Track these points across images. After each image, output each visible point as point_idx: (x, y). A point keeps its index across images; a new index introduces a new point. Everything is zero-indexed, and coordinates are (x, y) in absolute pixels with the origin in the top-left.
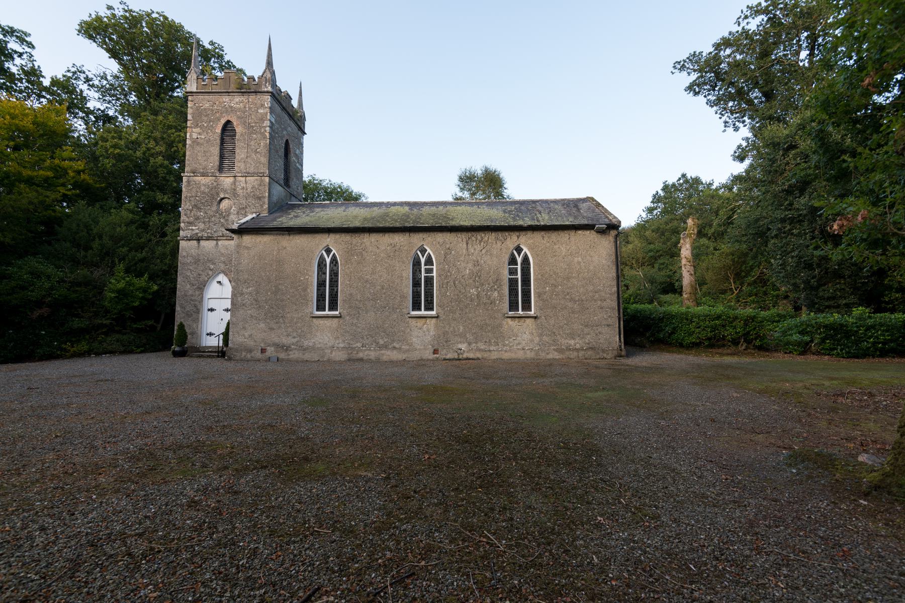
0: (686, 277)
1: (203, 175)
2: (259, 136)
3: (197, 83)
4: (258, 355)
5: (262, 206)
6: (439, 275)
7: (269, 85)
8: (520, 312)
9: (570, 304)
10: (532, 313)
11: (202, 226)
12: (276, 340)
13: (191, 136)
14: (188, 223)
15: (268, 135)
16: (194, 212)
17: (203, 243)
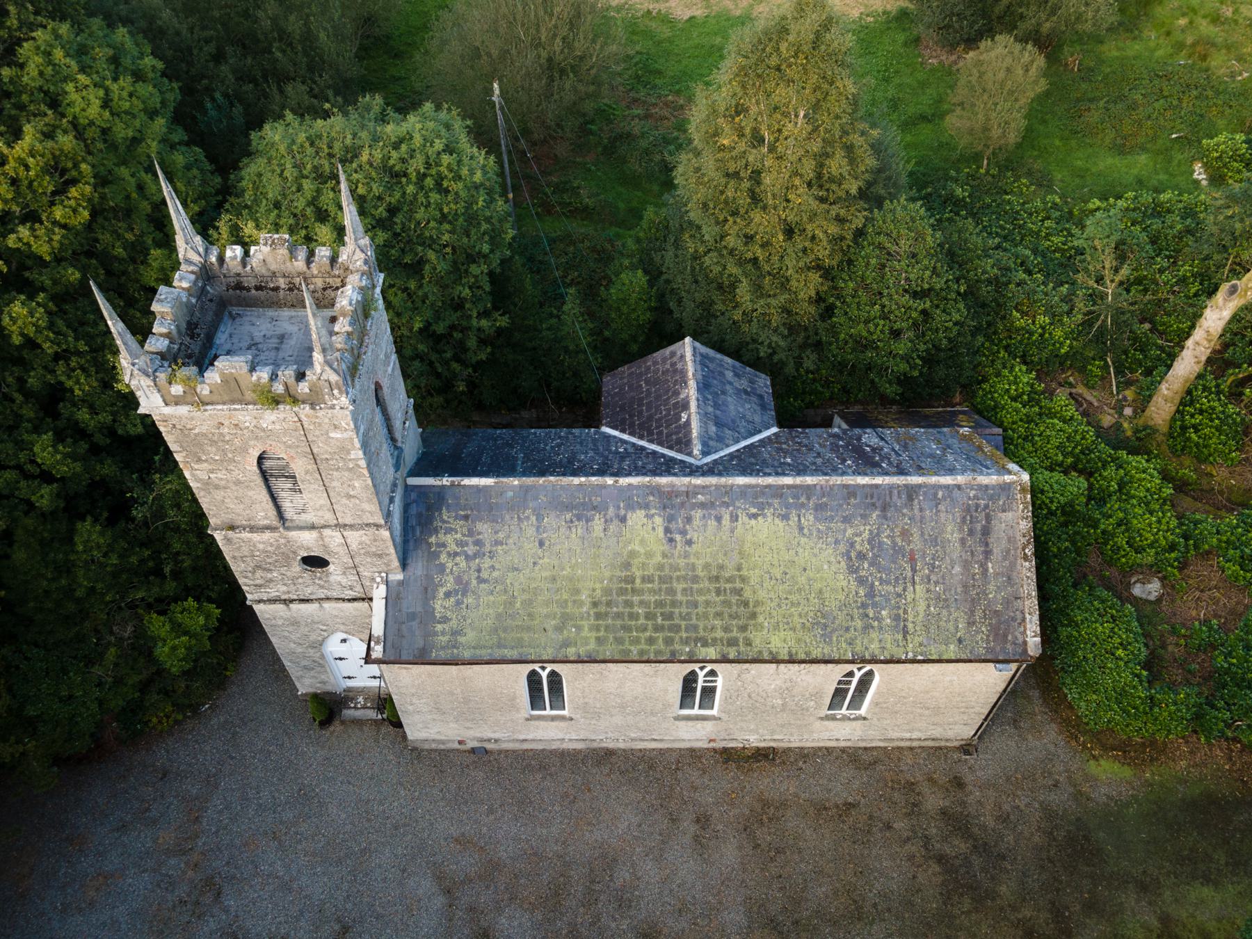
0: (1186, 361)
1: (253, 529)
2: (346, 474)
3: (159, 391)
4: (456, 746)
5: (387, 565)
6: (726, 689)
7: (341, 392)
8: (844, 711)
9: (919, 711)
10: (863, 711)
11: (285, 588)
12: (479, 735)
13: (193, 475)
14: (256, 586)
15: (366, 472)
16: (259, 573)
17: (293, 606)
